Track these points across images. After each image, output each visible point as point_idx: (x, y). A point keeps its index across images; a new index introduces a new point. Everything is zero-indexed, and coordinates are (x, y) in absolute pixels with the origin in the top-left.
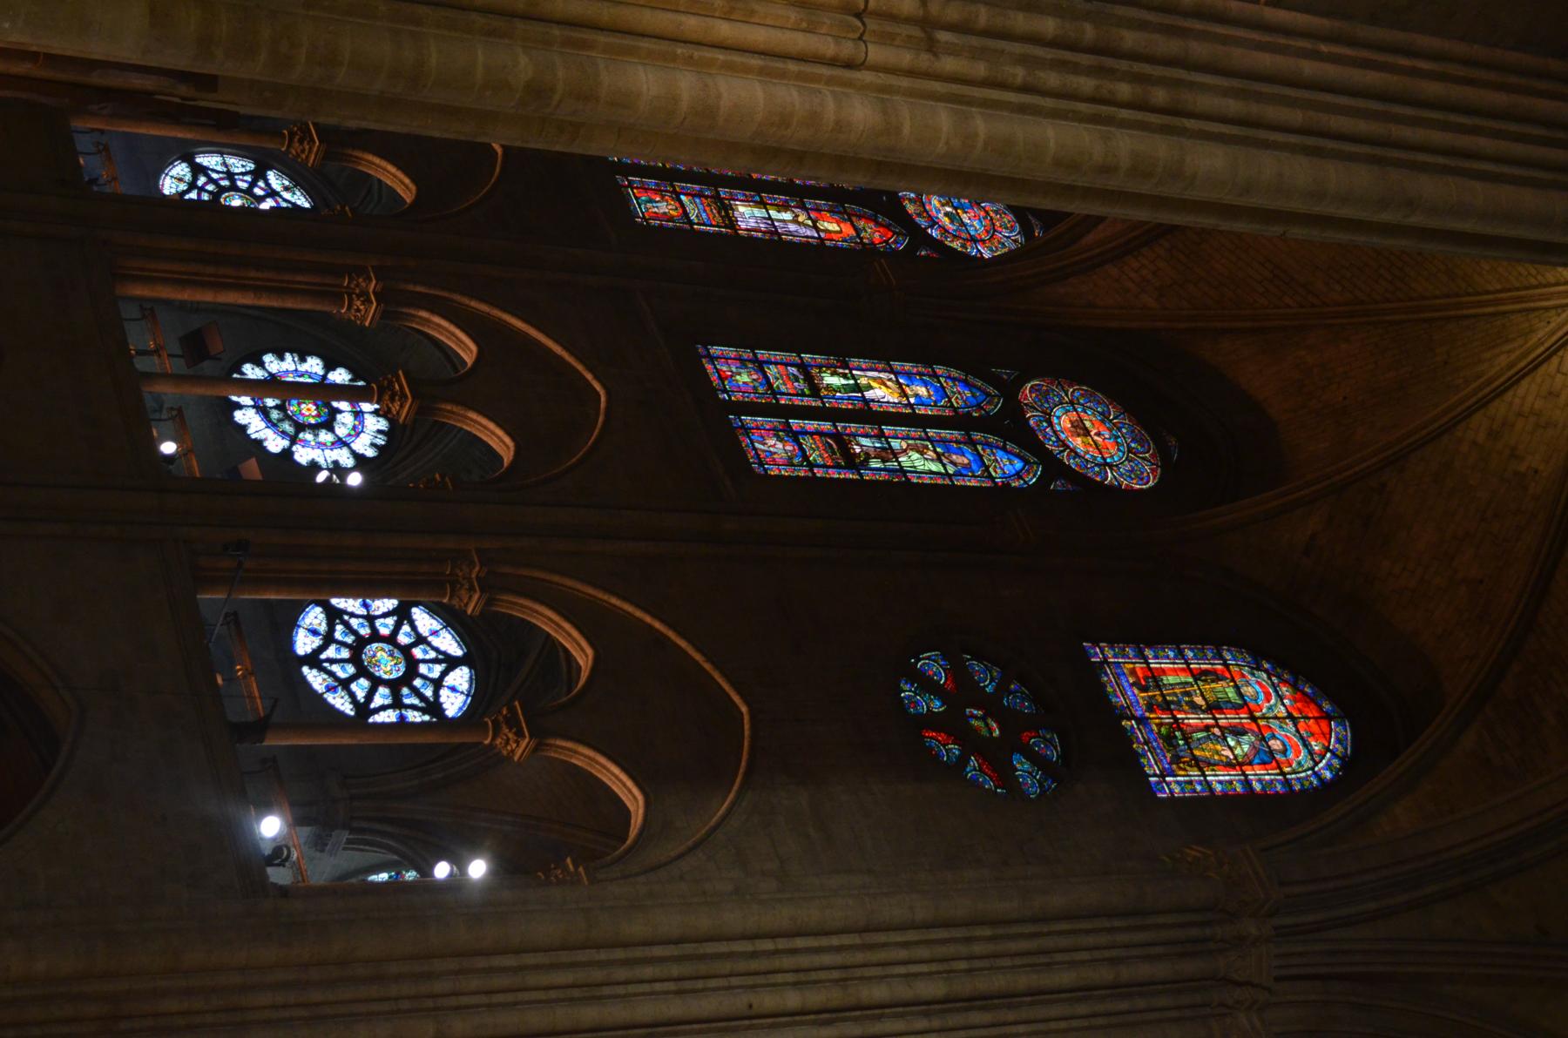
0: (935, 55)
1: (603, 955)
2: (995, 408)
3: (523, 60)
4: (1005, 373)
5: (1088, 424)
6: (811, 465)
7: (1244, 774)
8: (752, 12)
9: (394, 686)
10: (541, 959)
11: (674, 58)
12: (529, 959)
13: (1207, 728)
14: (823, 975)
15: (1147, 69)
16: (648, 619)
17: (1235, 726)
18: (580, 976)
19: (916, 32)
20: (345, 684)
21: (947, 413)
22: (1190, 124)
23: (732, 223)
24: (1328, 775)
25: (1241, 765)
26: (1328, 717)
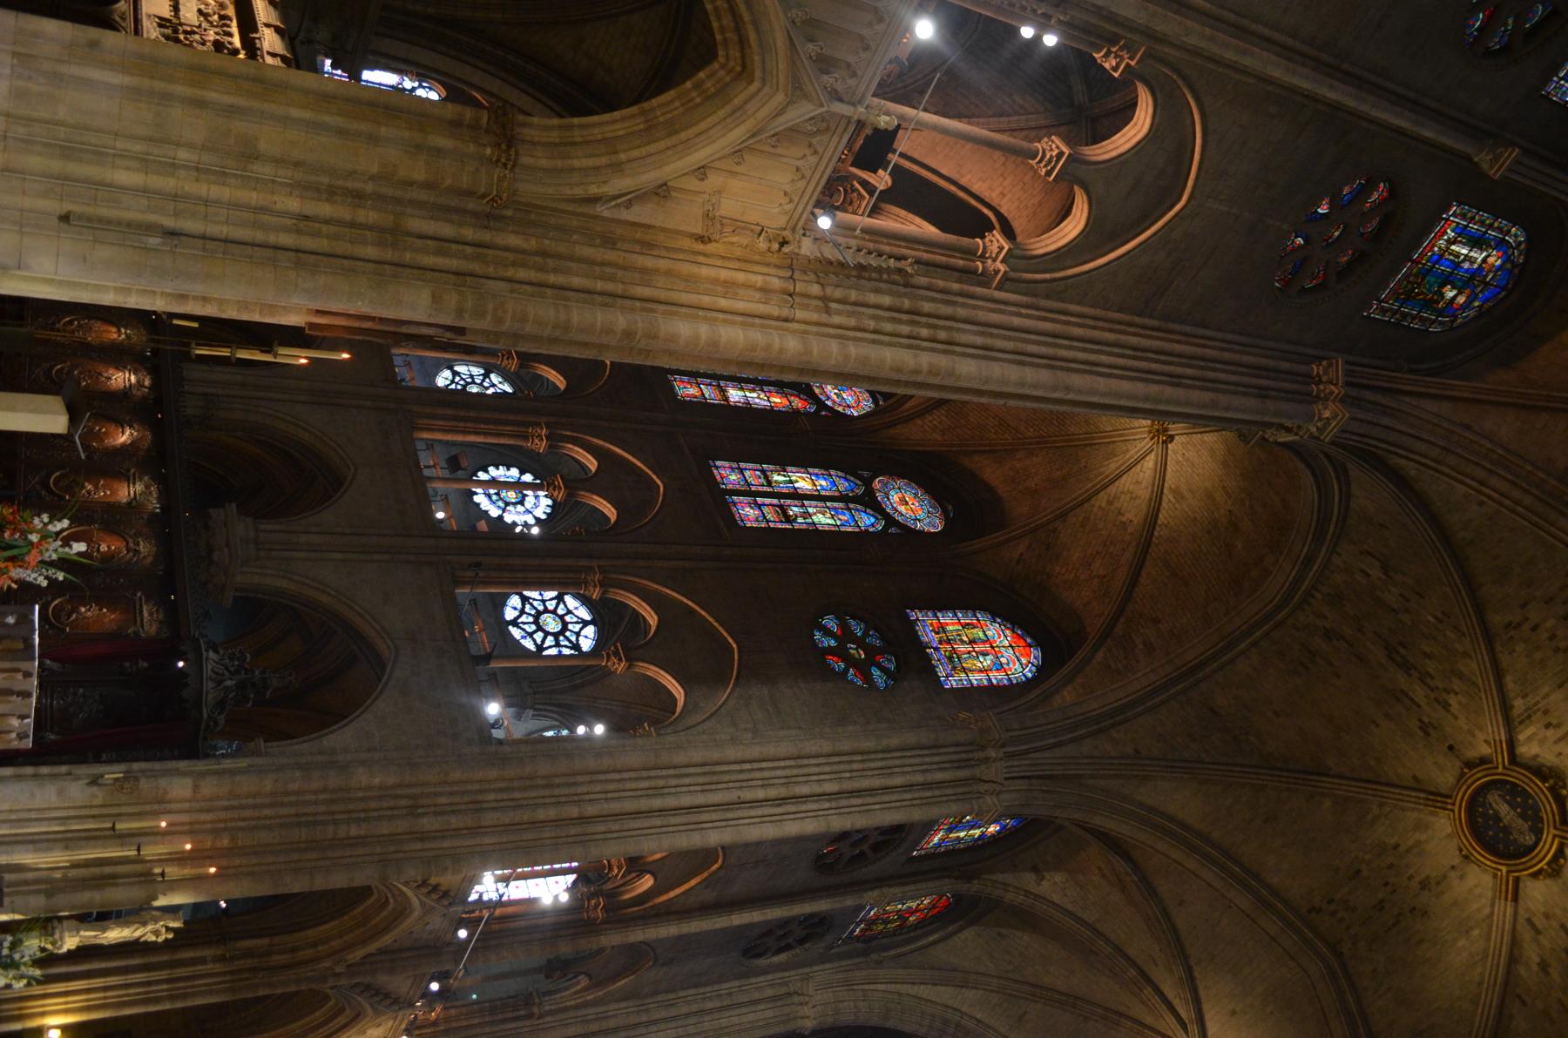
1: (664, 772)
2: (860, 491)
4: (866, 474)
9: (556, 635)
10: (633, 774)
11: (697, 317)
12: (626, 775)
15: (936, 321)
18: (653, 783)
19: (820, 303)
20: (531, 635)
22: (957, 349)
23: (727, 399)
26: (1030, 646)
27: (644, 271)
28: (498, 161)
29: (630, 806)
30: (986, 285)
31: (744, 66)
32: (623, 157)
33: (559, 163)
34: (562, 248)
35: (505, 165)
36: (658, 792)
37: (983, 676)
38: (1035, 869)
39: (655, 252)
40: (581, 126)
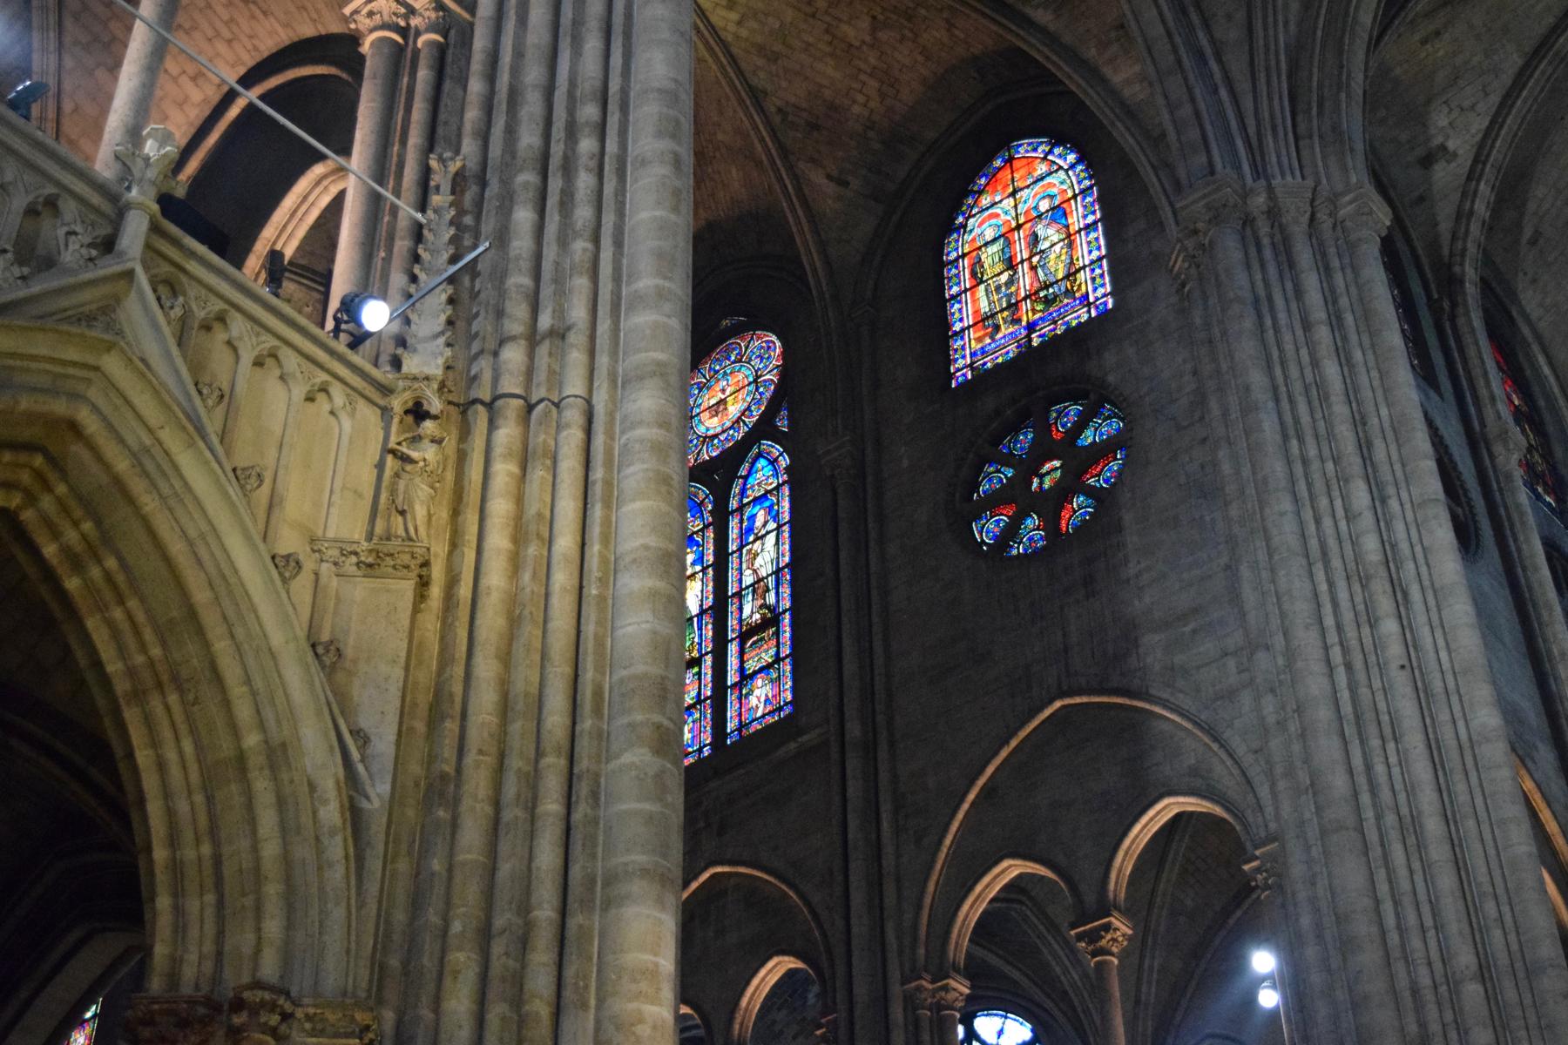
0: (569, 329)
1: (1369, 814)
3: (628, 758)
5: (713, 401)
6: (778, 659)
7: (1079, 231)
8: (540, 515)
10: (1381, 875)
12: (1383, 888)
13: (1033, 268)
14: (1359, 599)
16: (966, 806)
17: (1028, 245)
19: (543, 350)
21: (710, 534)
22: (615, 85)
24: (1072, 158)
25: (1069, 236)
26: (1010, 161)
27: (505, 707)
28: (274, 1032)
29: (1446, 881)
30: (467, 32)
31: (30, 447)
32: (252, 740)
33: (273, 890)
34: (469, 893)
35: (286, 1017)
36: (1412, 827)
37: (1081, 241)
38: (1427, 161)
39: (457, 689)
40: (173, 841)
